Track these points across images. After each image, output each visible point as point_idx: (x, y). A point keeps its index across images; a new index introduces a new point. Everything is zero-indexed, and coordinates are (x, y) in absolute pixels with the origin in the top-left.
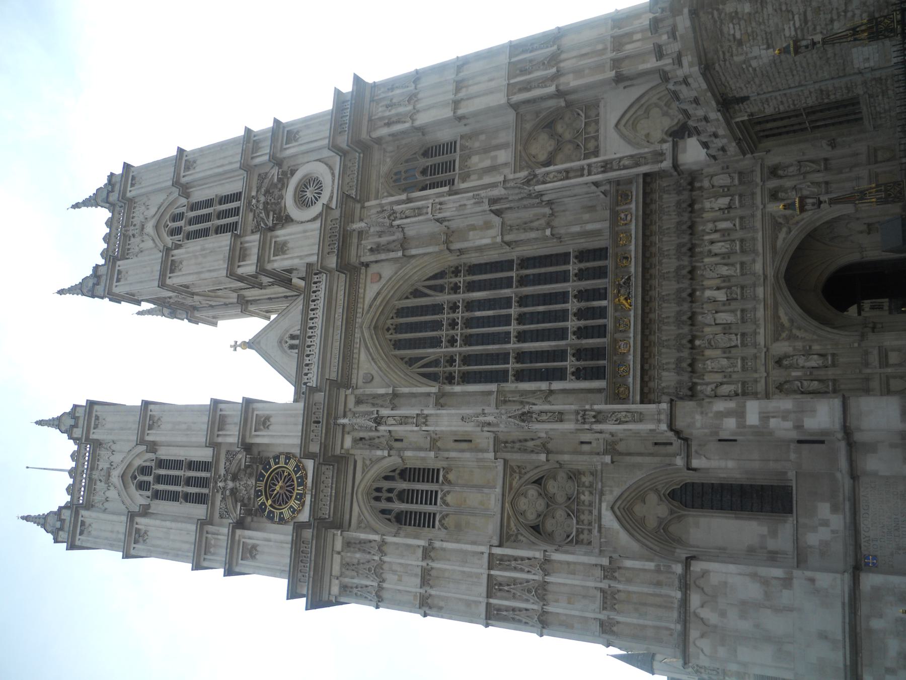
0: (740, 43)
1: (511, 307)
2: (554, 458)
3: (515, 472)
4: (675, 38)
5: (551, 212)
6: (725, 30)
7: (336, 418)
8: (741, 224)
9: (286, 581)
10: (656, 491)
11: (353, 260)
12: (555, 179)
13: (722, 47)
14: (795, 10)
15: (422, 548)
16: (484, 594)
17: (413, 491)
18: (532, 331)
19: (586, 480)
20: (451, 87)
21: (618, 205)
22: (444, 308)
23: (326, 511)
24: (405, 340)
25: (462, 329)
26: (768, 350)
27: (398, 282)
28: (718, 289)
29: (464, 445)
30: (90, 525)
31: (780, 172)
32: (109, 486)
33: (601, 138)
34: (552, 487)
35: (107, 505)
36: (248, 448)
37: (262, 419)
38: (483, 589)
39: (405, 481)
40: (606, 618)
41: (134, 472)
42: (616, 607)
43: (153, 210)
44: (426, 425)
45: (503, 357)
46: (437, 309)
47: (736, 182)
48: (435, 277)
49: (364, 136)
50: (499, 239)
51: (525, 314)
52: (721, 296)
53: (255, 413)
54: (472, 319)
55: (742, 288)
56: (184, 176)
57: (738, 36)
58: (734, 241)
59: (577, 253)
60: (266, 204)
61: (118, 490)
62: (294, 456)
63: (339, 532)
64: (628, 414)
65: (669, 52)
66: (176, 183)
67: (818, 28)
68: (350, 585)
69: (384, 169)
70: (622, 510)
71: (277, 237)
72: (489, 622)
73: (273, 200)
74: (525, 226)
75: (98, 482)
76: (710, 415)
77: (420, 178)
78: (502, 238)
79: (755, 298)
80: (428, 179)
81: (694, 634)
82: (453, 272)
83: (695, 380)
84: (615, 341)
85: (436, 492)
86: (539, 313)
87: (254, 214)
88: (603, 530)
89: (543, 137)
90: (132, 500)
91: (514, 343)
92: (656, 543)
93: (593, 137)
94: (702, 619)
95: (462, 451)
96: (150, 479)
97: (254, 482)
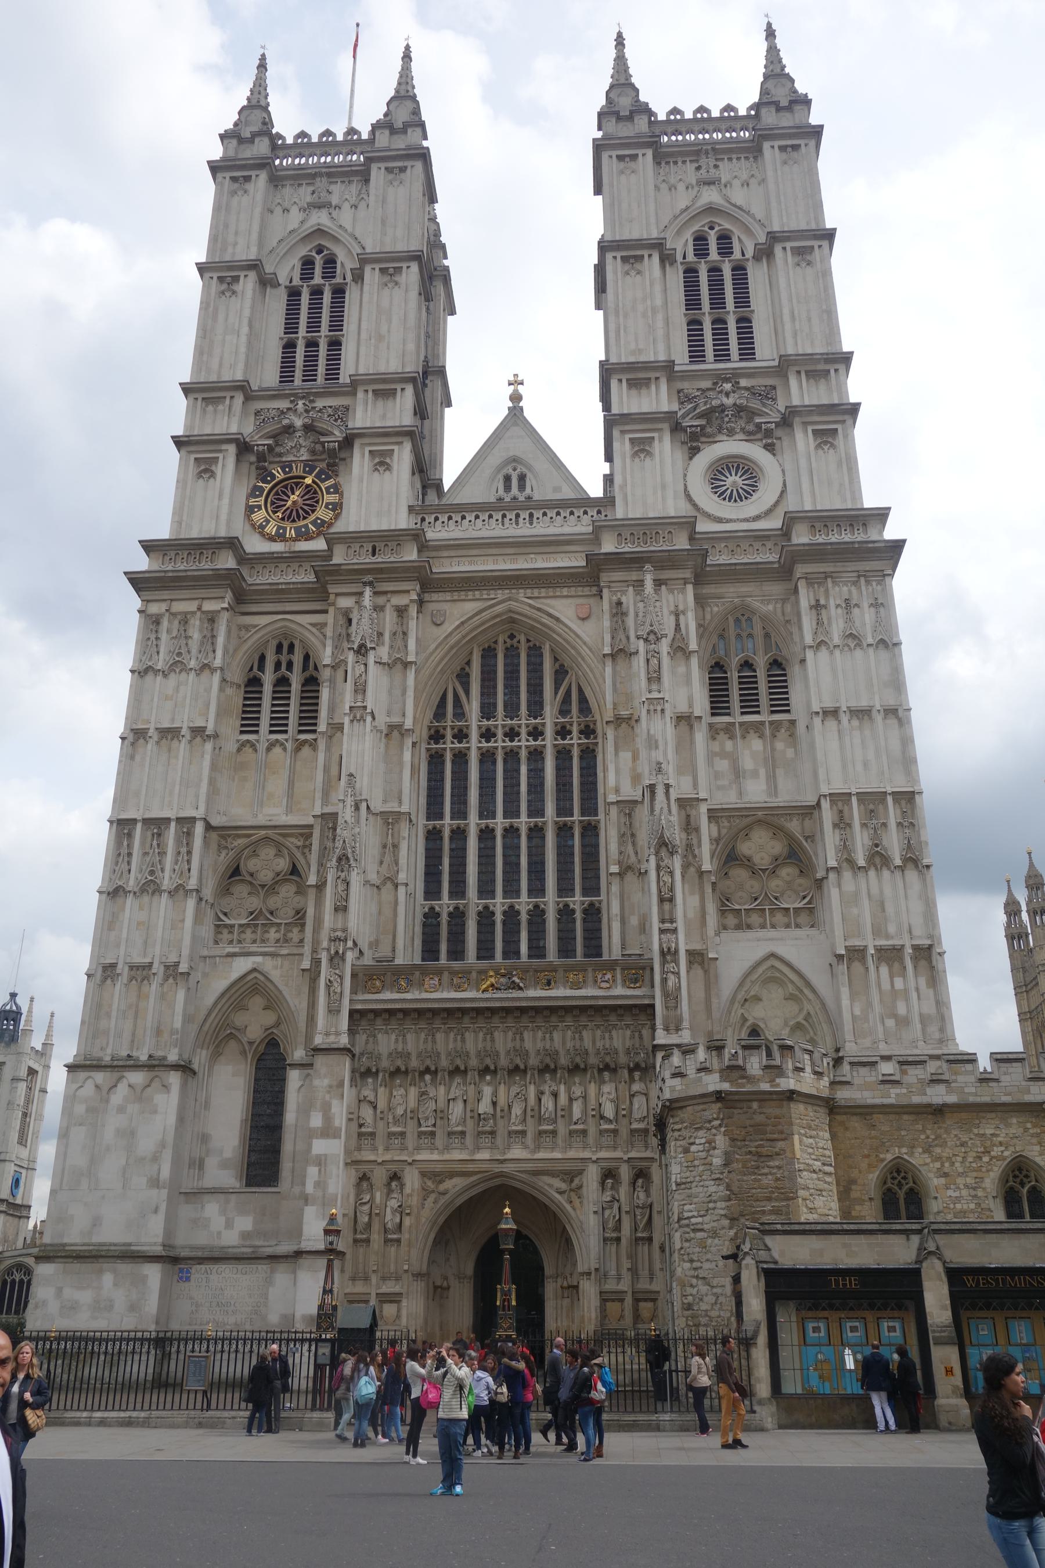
0: (686, 1151)
1: (529, 816)
2: (312, 894)
3: (306, 839)
4: (699, 1070)
5: (642, 871)
6: (701, 1133)
7: (371, 584)
8: (576, 1131)
9: (167, 537)
10: (277, 1024)
11: (605, 577)
12: (662, 884)
13: (686, 1128)
14: (707, 1219)
15: (203, 725)
16: (146, 816)
17: (289, 698)
18: (494, 848)
19: (295, 935)
20: (864, 703)
21: (623, 969)
22: (535, 718)
23: (258, 579)
24: (496, 666)
25: (503, 748)
26: (410, 1164)
27: (574, 648)
28: (494, 1104)
29: (334, 771)
30: (245, 192)
31: (640, 1181)
32: (305, 210)
33: (762, 933)
34: (287, 891)
35: (278, 210)
36: (348, 442)
37: (388, 460)
38: (155, 813)
39: (303, 685)
40: (118, 971)
41: (328, 249)
42: (134, 982)
43: (738, 196)
44: (352, 721)
45: (460, 811)
46: (536, 708)
47: (635, 1126)
48: (583, 700)
49: (800, 570)
50: (612, 798)
51: (519, 837)
52: (484, 1107)
53: (396, 448)
54: (519, 760)
55: (493, 1133)
56: (784, 249)
57: (693, 1148)
58: (555, 1122)
59: (597, 905)
60: (722, 408)
61: (299, 228)
62: (337, 517)
63: (226, 605)
64: (337, 997)
65: (687, 1062)
66: (774, 238)
67: (687, 1245)
68: (160, 627)
69: (755, 604)
70: (255, 981)
71: (661, 440)
72: (115, 825)
73: (726, 419)
74: (628, 835)
75: (312, 188)
76: (327, 1097)
77: (734, 662)
78: (612, 803)
79: (478, 1148)
80: (734, 676)
81: (99, 1077)
82: (587, 726)
83: (381, 1075)
84: (439, 972)
85: (286, 732)
86: (519, 856)
87: (708, 389)
88: (229, 959)
89: (778, 847)
90: (285, 254)
91: (478, 825)
92: (214, 1025)
93: (765, 920)
94: (116, 1086)
95: (327, 769)
96: (318, 280)
97: (304, 458)
